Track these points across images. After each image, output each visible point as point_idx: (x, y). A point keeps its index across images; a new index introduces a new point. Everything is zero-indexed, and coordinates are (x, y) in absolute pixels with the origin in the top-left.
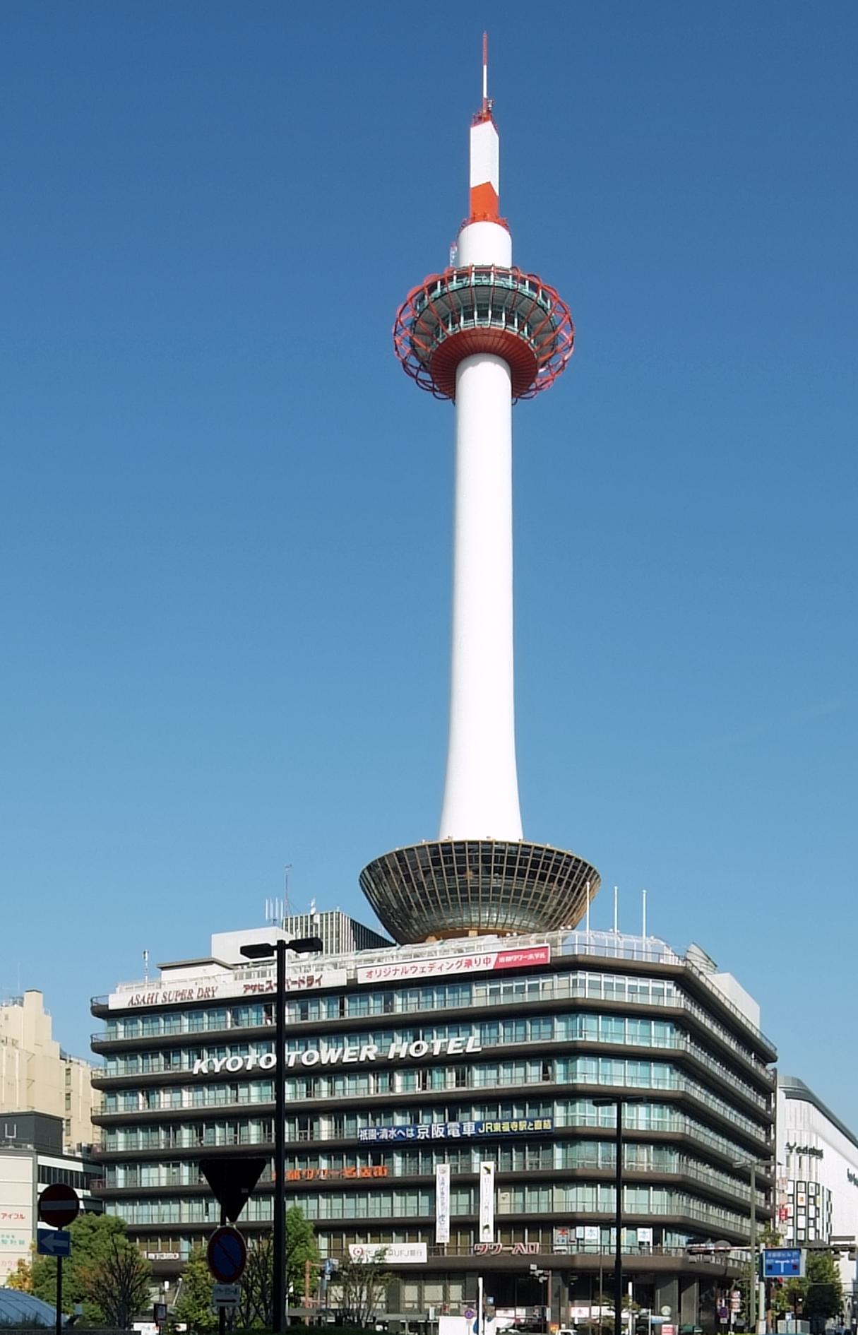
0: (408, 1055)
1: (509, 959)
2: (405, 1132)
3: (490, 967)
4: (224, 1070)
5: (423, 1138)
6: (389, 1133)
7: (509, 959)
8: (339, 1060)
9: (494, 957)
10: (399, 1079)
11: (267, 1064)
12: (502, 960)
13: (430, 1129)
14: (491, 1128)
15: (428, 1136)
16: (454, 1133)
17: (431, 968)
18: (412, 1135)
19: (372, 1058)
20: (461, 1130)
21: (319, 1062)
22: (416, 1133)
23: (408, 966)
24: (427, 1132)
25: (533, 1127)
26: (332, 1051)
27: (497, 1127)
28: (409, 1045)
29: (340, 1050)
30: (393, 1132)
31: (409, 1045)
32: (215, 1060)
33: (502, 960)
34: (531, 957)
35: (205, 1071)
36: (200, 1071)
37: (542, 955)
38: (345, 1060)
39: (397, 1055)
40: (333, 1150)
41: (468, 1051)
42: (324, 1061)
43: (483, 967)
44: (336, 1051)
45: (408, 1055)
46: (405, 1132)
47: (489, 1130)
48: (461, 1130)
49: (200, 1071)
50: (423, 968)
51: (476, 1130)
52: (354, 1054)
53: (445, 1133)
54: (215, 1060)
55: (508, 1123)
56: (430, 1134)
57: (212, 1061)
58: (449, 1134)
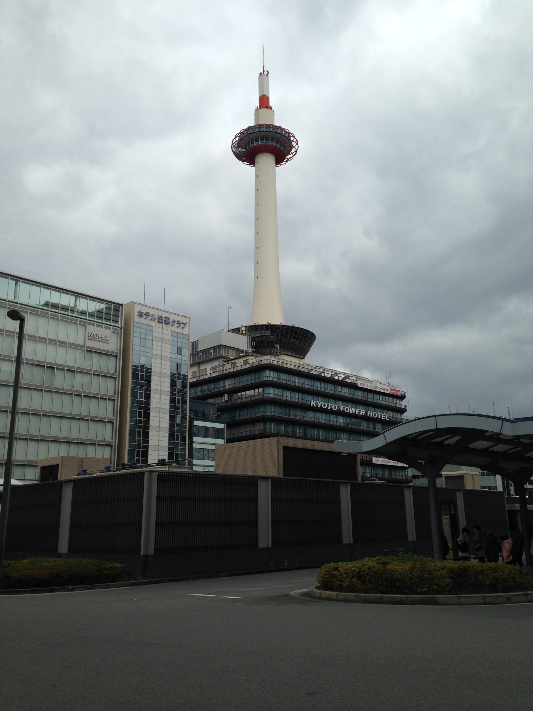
7: (393, 391)
8: (355, 413)
11: (335, 409)
19: (364, 415)
28: (373, 413)
29: (355, 409)
31: (373, 413)
32: (318, 402)
34: (397, 392)
35: (315, 406)
36: (313, 405)
37: (399, 393)
39: (370, 415)
43: (387, 392)
44: (354, 409)
49: (313, 405)
50: (374, 387)
52: (359, 412)
57: (317, 402)
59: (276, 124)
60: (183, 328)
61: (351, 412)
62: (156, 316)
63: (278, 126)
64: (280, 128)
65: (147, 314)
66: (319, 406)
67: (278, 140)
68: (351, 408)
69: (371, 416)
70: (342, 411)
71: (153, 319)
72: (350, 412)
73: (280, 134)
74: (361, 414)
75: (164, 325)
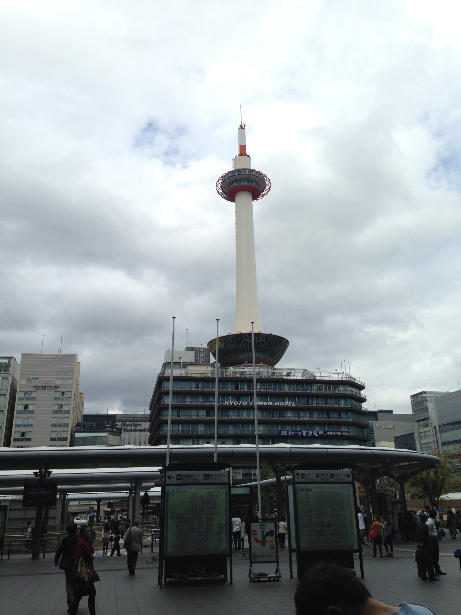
2: (298, 433)
5: (304, 435)
6: (292, 433)
10: (302, 414)
13: (307, 433)
14: (328, 434)
15: (306, 435)
16: (316, 434)
18: (301, 434)
24: (306, 433)
25: (343, 434)
27: (331, 434)
30: (293, 433)
41: (293, 405)
46: (298, 433)
47: (328, 434)
51: (323, 434)
53: (313, 434)
55: (334, 433)
56: (307, 434)
58: (314, 435)
59: (252, 168)
63: (253, 170)
64: (255, 170)
67: (253, 180)
73: (255, 175)
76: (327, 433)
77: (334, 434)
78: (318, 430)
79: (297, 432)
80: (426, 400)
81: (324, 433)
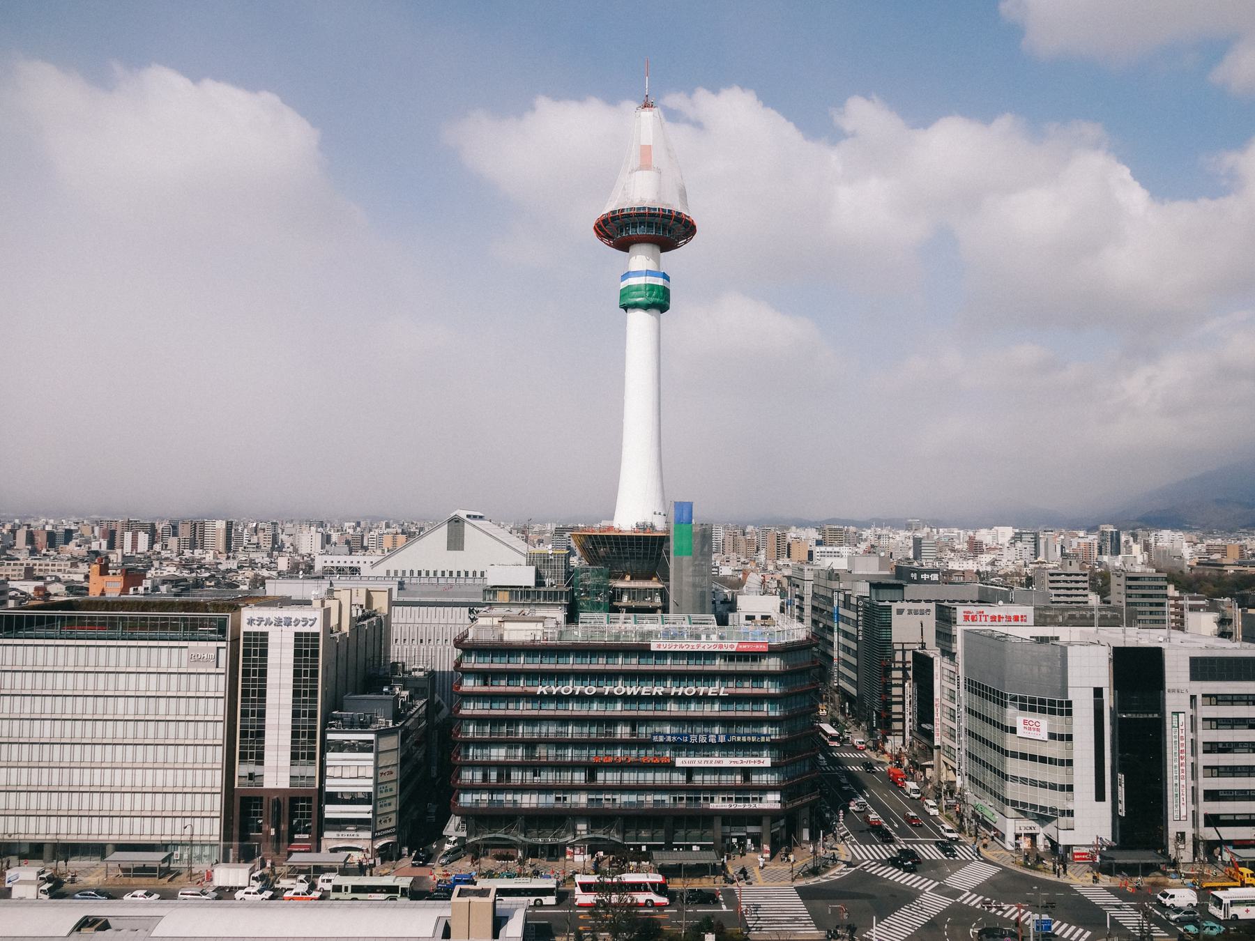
0: (683, 693)
1: (745, 647)
3: (734, 650)
4: (559, 693)
7: (745, 647)
9: (736, 645)
12: (740, 646)
13: (698, 737)
16: (712, 740)
17: (698, 646)
20: (717, 739)
21: (626, 693)
22: (689, 739)
23: (684, 644)
26: (634, 688)
30: (674, 738)
33: (740, 646)
35: (545, 693)
36: (542, 692)
38: (643, 694)
40: (626, 744)
42: (629, 693)
45: (683, 693)
48: (717, 739)
49: (542, 692)
53: (707, 740)
54: (553, 687)
56: (698, 740)
60: (311, 626)
61: (629, 693)
62: (272, 619)
65: (260, 620)
66: (554, 693)
68: (628, 688)
69: (680, 694)
70: (606, 693)
71: (269, 623)
72: (626, 693)
74: (654, 694)
75: (284, 628)
76: (733, 738)
77: (744, 739)
78: (717, 732)
79: (682, 736)
80: (955, 622)
81: (728, 737)
